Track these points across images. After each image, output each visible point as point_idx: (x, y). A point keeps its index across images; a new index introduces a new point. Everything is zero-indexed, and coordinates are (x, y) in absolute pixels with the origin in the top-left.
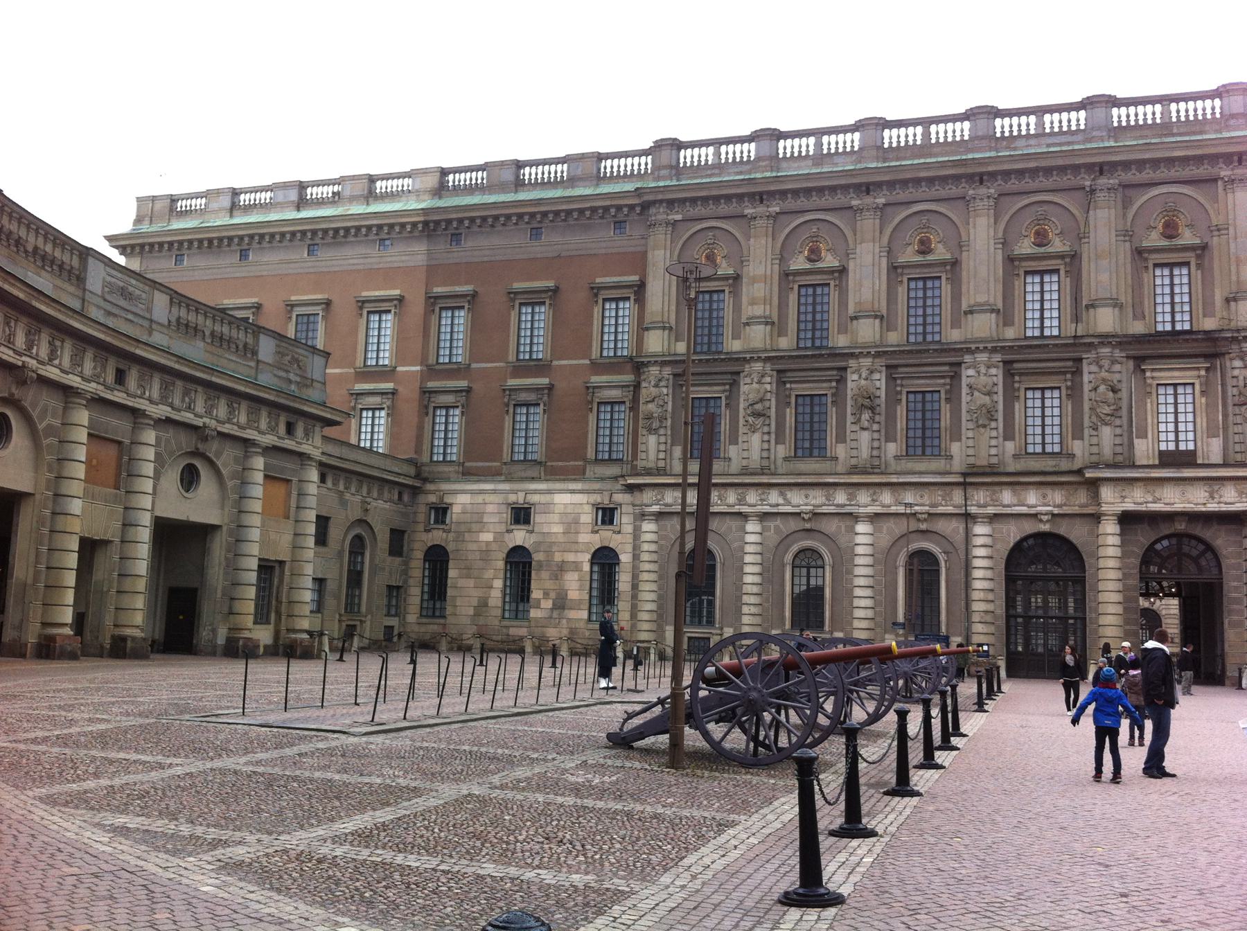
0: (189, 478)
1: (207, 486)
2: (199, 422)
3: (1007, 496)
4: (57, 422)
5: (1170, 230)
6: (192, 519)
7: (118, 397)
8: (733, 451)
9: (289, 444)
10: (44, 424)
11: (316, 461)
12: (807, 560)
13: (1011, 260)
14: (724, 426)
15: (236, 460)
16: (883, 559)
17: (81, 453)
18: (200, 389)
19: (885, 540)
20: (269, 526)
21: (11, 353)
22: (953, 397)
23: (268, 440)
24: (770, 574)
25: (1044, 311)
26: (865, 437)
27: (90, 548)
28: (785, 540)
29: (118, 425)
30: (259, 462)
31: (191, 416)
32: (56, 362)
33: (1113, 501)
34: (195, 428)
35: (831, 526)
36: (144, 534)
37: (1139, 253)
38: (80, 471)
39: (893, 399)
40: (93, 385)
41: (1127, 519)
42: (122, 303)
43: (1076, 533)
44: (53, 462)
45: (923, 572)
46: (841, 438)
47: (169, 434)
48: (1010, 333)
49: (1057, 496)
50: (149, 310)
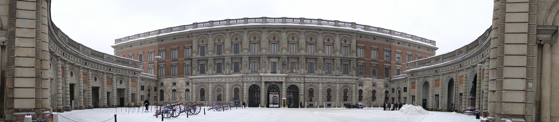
0: (121, 82)
1: (123, 83)
3: (249, 79)
5: (274, 38)
7: (110, 72)
8: (207, 72)
12: (219, 90)
13: (250, 42)
14: (206, 68)
16: (230, 90)
19: (231, 86)
20: (132, 89)
22: (241, 63)
24: (213, 92)
25: (255, 50)
26: (228, 69)
27: (108, 93)
28: (216, 87)
29: (111, 76)
30: (130, 79)
33: (264, 80)
35: (222, 84)
36: (115, 91)
37: (270, 41)
38: (106, 83)
39: (232, 63)
41: (266, 82)
43: (259, 85)
45: (236, 91)
46: (224, 70)
47: (117, 76)
48: (250, 54)
49: (256, 79)
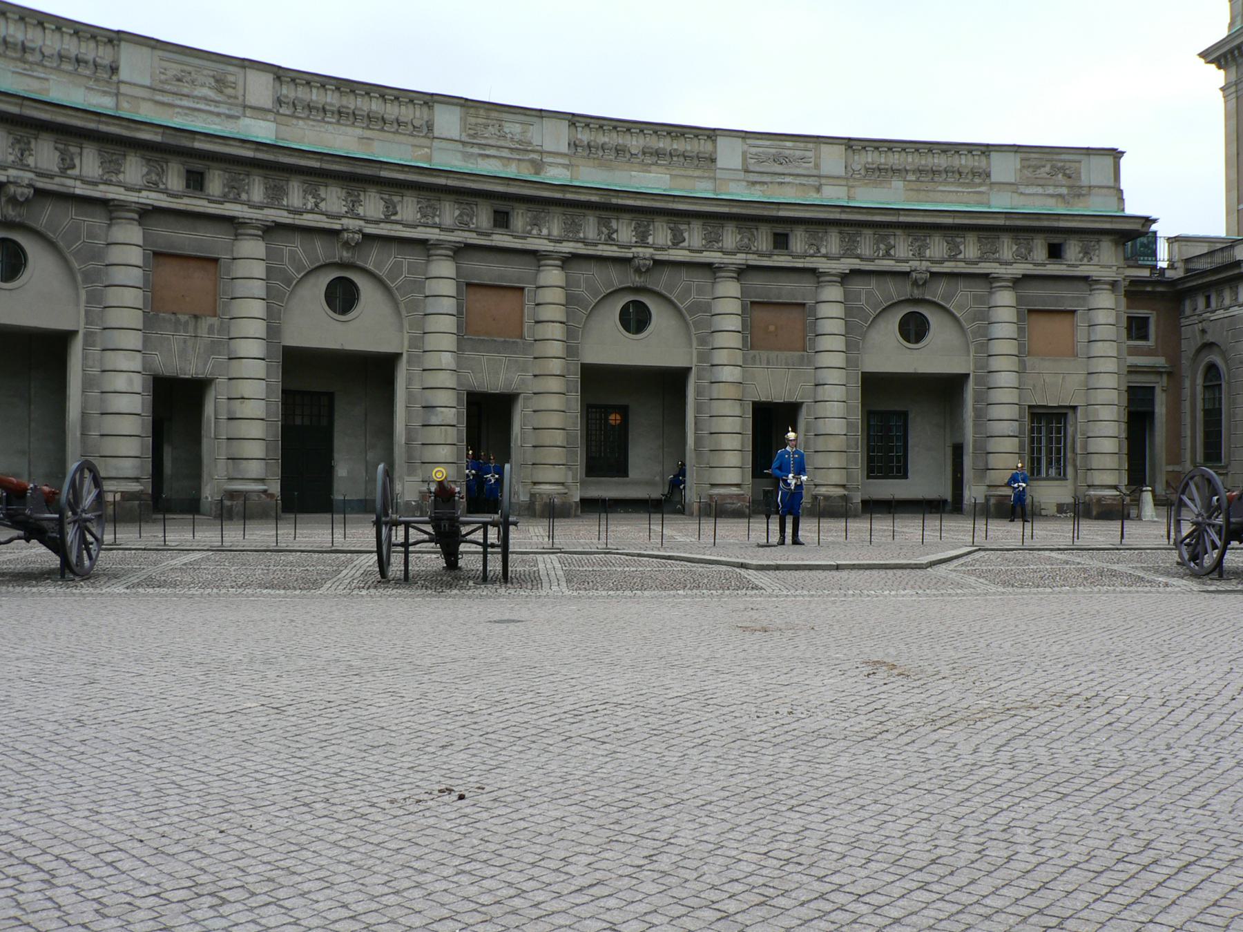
2: (905, 267)
4: (702, 299)
6: (920, 371)
9: (1054, 269)
10: (688, 303)
11: (1106, 283)
15: (979, 299)
17: (734, 323)
18: (899, 232)
21: (615, 248)
23: (1019, 269)
30: (1005, 298)
31: (892, 262)
32: (685, 244)
34: (906, 274)
40: (740, 256)
42: (778, 169)
44: (705, 337)
50: (817, 166)
